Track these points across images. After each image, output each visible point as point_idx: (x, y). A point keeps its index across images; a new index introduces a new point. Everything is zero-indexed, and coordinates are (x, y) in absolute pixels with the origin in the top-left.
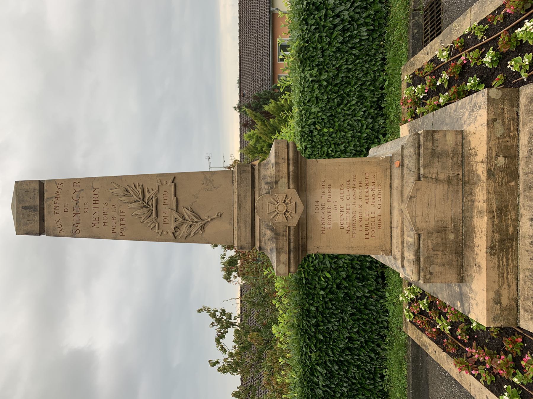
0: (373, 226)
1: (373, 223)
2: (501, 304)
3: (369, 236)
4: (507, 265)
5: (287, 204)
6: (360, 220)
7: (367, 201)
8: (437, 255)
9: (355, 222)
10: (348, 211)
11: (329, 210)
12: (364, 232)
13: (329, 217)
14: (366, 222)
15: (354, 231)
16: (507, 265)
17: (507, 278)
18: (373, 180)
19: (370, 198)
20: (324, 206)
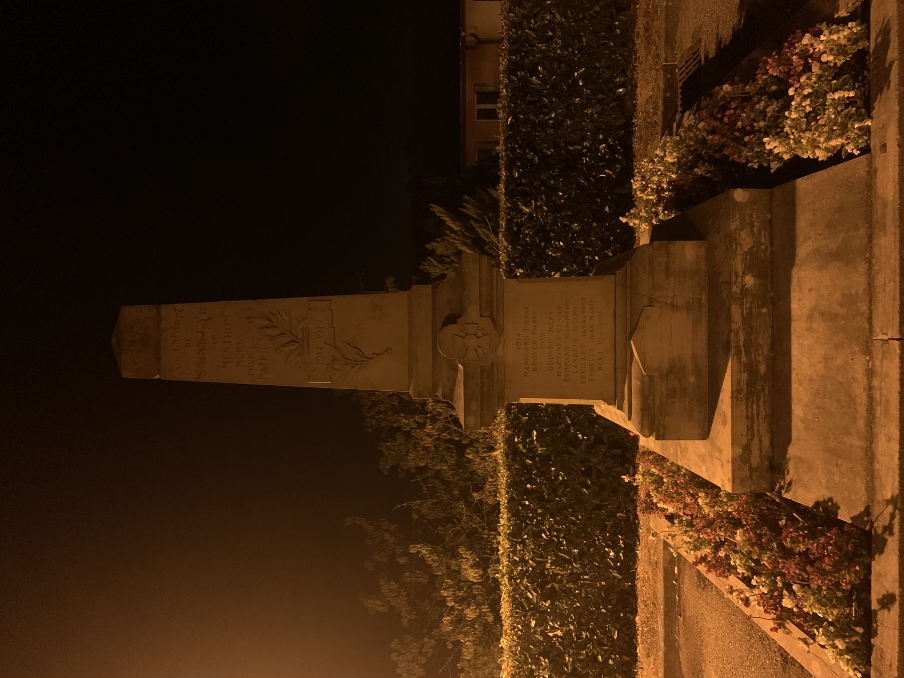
2: (750, 465)
4: (758, 414)
7: (584, 334)
8: (673, 403)
10: (559, 347)
16: (758, 414)
17: (758, 431)
20: (527, 341)
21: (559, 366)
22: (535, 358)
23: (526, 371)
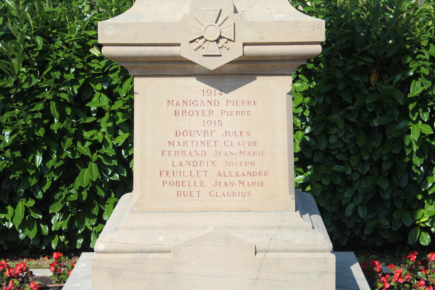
0: (181, 183)
1: (186, 184)
3: (164, 178)
5: (217, 41)
6: (191, 164)
7: (222, 174)
9: (187, 155)
10: (206, 144)
11: (207, 113)
12: (171, 169)
13: (195, 114)
14: (187, 173)
15: (173, 154)
18: (257, 184)
19: (228, 180)
20: (213, 104)
21: (182, 144)
22: (191, 113)
23: (175, 103)
